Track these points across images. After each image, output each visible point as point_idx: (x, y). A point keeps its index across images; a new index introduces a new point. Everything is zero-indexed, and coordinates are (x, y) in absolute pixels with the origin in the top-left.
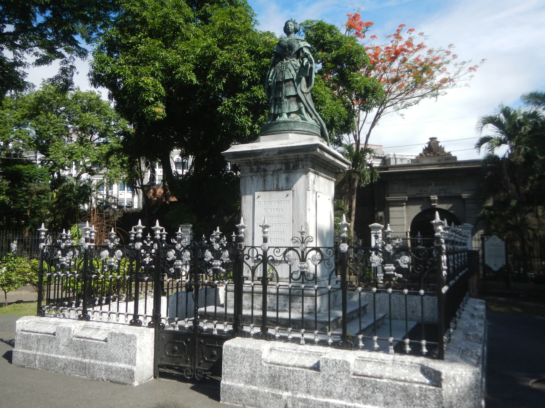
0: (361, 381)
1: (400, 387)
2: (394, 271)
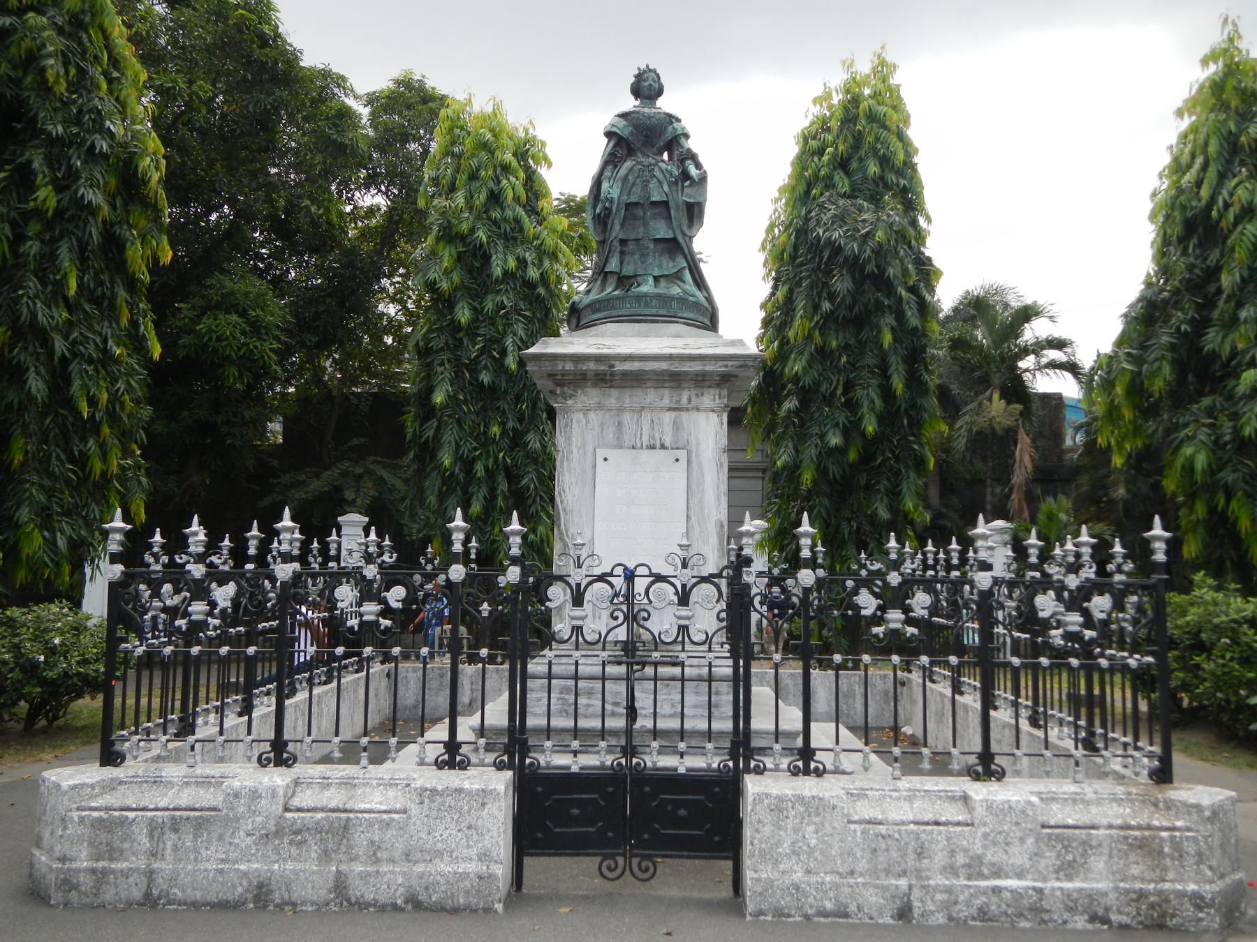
0: (1059, 838)
1: (1136, 838)
2: (1080, 626)
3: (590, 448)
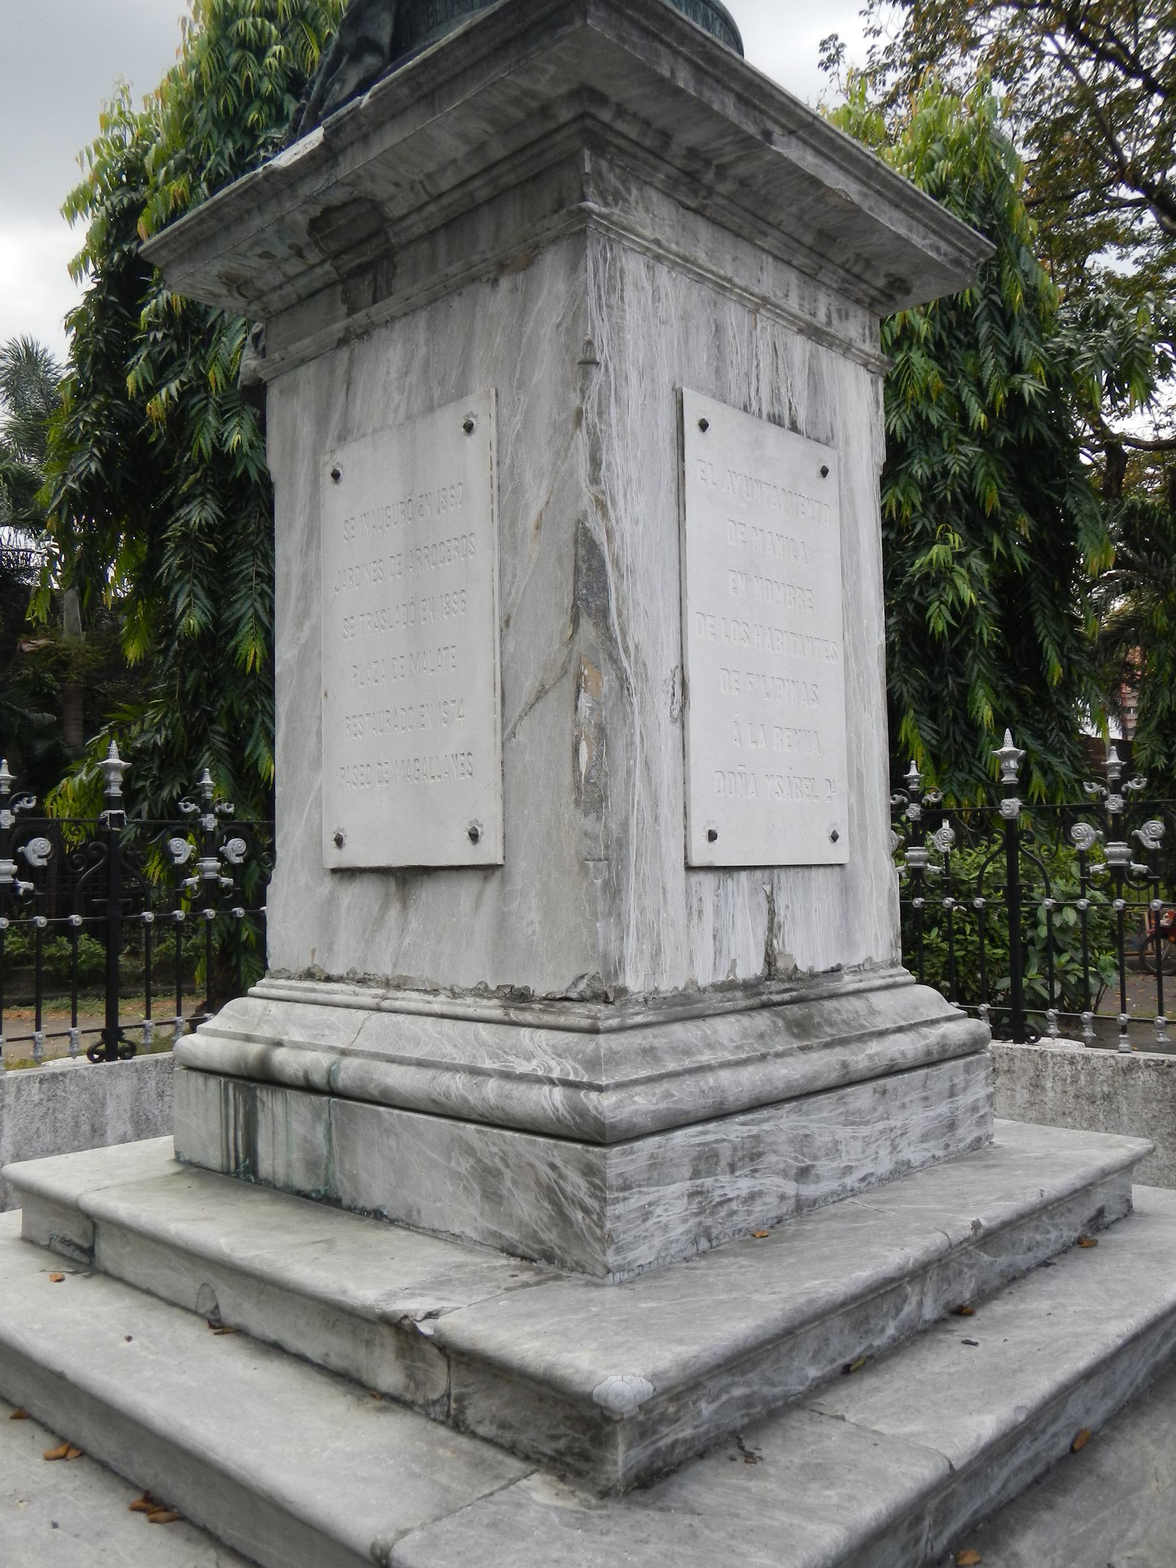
3: (665, 380)
